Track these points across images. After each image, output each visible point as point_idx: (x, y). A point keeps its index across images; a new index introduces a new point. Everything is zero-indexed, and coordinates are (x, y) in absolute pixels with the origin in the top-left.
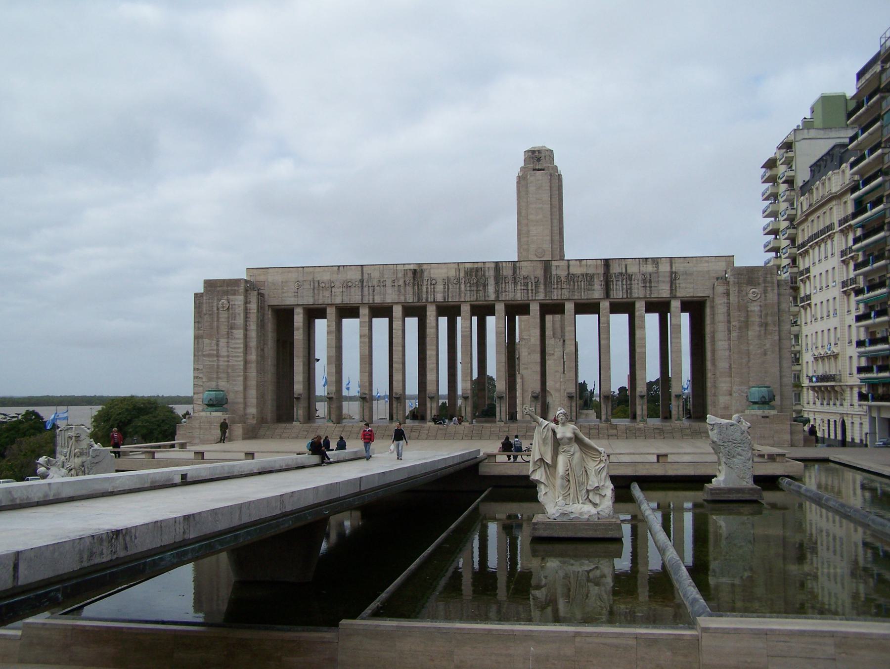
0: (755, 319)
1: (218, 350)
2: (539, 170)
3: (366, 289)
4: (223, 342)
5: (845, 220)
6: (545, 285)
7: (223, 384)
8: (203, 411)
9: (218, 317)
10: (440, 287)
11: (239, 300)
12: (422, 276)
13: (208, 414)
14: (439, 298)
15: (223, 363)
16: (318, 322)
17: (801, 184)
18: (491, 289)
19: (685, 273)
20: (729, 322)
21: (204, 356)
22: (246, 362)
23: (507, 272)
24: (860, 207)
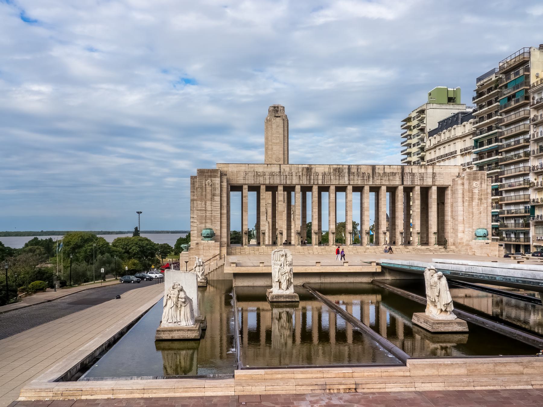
0: (476, 197)
1: (206, 207)
2: (277, 117)
3: (282, 177)
4: (208, 203)
5: (466, 149)
6: (373, 178)
7: (209, 226)
8: (202, 240)
9: (206, 190)
10: (320, 177)
11: (217, 180)
12: (311, 172)
13: (207, 242)
14: (320, 182)
15: (208, 214)
16: (309, 194)
17: (428, 131)
18: (346, 178)
19: (440, 173)
20: (463, 198)
21: (197, 210)
22: (221, 214)
23: (354, 170)
24: (479, 143)
